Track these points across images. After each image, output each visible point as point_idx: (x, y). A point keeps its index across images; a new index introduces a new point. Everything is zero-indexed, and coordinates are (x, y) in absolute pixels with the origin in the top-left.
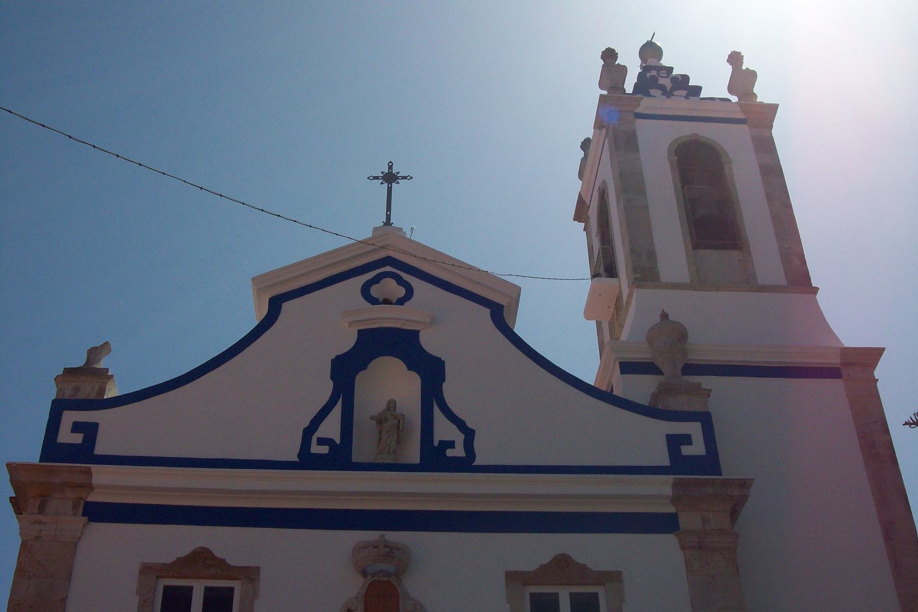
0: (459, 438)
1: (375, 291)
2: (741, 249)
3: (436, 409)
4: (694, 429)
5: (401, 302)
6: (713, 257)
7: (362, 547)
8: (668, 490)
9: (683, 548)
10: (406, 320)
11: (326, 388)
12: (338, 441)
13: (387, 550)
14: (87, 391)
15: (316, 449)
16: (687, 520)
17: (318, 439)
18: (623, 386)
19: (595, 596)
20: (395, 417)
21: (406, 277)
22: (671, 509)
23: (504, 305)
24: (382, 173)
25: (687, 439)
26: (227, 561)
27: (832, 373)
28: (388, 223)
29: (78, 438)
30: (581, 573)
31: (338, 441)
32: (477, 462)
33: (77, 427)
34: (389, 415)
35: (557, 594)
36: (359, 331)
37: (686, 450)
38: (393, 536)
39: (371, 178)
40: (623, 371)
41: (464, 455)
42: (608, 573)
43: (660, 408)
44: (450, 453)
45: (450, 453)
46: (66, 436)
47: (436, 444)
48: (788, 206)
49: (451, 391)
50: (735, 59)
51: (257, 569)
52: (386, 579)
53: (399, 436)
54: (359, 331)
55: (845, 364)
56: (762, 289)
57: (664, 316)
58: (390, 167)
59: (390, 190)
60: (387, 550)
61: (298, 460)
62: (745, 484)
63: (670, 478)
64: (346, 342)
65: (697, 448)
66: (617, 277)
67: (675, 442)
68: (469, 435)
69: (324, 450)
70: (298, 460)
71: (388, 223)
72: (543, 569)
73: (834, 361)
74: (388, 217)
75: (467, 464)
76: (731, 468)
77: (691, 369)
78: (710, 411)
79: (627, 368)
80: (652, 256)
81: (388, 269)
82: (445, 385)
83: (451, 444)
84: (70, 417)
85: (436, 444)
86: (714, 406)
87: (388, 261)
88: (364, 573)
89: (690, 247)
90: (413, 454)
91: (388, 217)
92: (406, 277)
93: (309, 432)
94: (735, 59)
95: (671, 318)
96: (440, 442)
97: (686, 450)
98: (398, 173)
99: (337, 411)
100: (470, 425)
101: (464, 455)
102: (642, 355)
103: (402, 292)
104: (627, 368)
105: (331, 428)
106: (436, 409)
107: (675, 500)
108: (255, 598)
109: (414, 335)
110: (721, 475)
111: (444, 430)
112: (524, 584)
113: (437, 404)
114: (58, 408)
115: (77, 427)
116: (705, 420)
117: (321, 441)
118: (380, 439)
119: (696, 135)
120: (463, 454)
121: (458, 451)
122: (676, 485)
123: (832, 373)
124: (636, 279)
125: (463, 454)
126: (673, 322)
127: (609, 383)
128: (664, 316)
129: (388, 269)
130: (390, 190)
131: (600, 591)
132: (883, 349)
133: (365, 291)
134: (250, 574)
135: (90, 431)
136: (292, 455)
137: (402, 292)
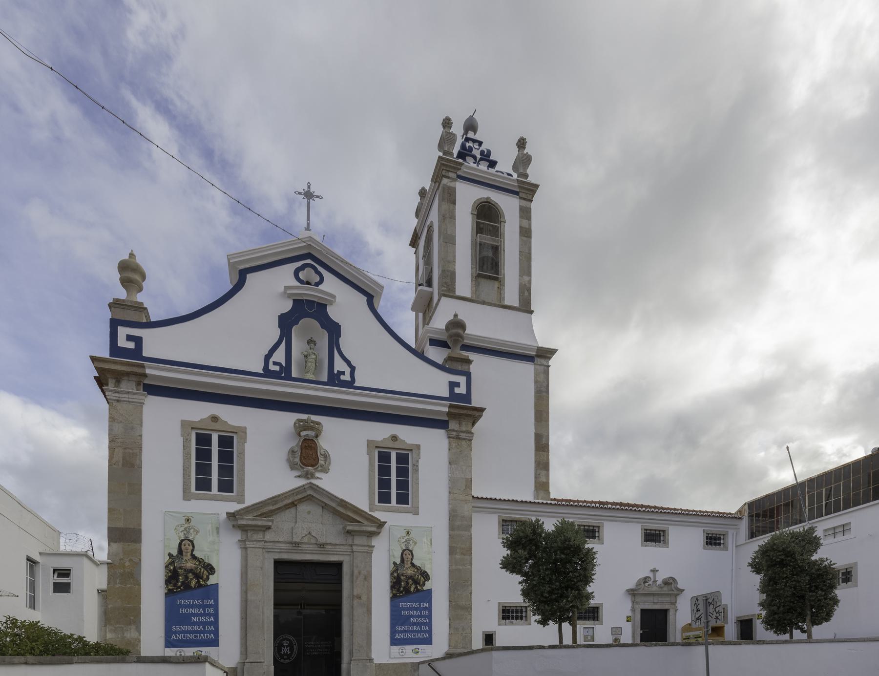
0: (348, 370)
4: (462, 380)
11: (276, 333)
12: (284, 365)
15: (272, 367)
22: (447, 419)
25: (458, 385)
29: (131, 345)
33: (129, 338)
37: (457, 390)
44: (342, 377)
45: (342, 377)
46: (122, 343)
47: (336, 372)
61: (263, 372)
65: (461, 390)
67: (453, 385)
68: (353, 369)
69: (277, 368)
70: (263, 372)
75: (350, 384)
83: (343, 373)
84: (123, 332)
85: (336, 372)
93: (268, 357)
96: (338, 371)
97: (457, 390)
99: (283, 346)
105: (280, 356)
111: (339, 365)
114: (114, 324)
115: (129, 338)
116: (468, 375)
117: (275, 363)
120: (350, 380)
121: (347, 377)
125: (350, 380)
135: (138, 341)
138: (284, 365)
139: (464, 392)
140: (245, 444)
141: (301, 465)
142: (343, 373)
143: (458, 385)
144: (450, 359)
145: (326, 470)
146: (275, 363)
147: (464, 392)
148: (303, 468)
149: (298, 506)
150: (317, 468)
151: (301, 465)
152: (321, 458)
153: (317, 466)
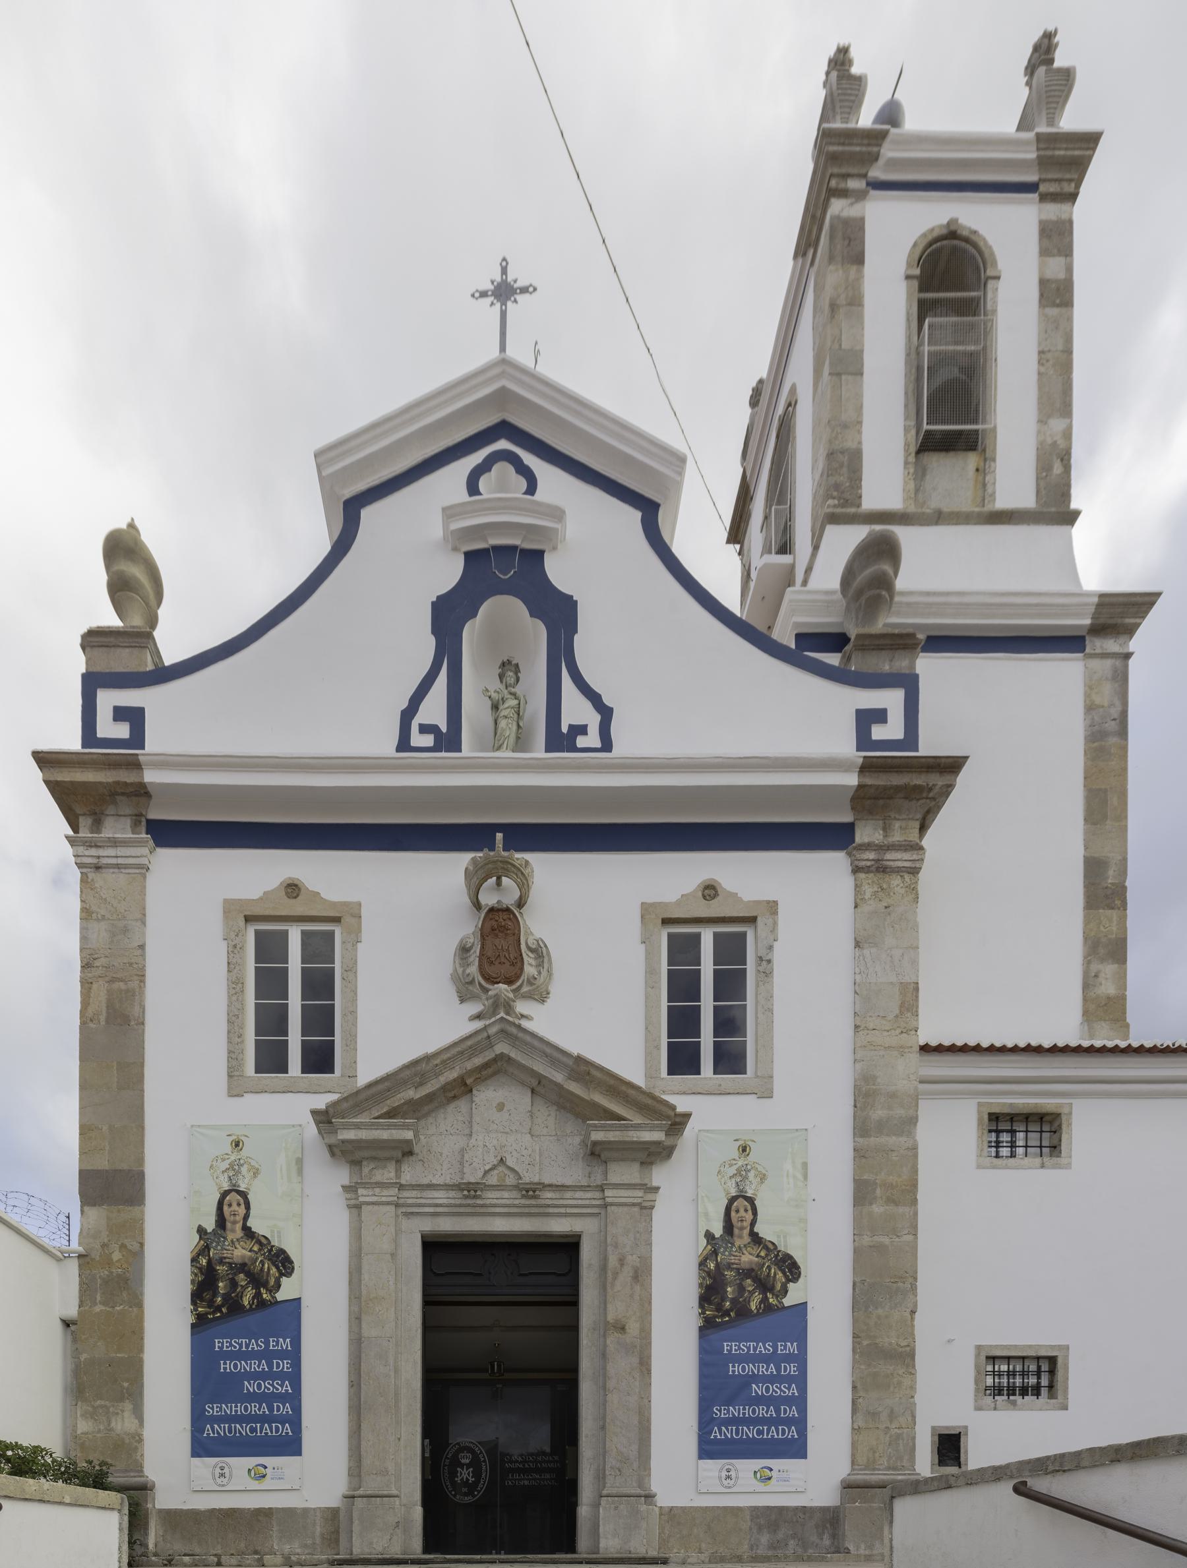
0: (593, 720)
11: (427, 646)
12: (444, 728)
14: (123, 660)
21: (529, 459)
25: (880, 716)
26: (322, 895)
31: (444, 729)
33: (120, 714)
37: (878, 733)
44: (581, 742)
47: (565, 729)
49: (584, 646)
59: (503, 315)
67: (867, 718)
68: (606, 713)
81: (503, 444)
82: (576, 637)
84: (107, 700)
85: (565, 729)
92: (529, 459)
93: (407, 715)
96: (571, 727)
97: (878, 733)
100: (607, 701)
114: (92, 683)
115: (120, 714)
117: (424, 729)
130: (503, 315)
132: (1158, 595)
138: (444, 729)
141: (483, 982)
142: (582, 730)
143: (880, 716)
145: (541, 996)
146: (424, 729)
148: (486, 991)
152: (528, 959)
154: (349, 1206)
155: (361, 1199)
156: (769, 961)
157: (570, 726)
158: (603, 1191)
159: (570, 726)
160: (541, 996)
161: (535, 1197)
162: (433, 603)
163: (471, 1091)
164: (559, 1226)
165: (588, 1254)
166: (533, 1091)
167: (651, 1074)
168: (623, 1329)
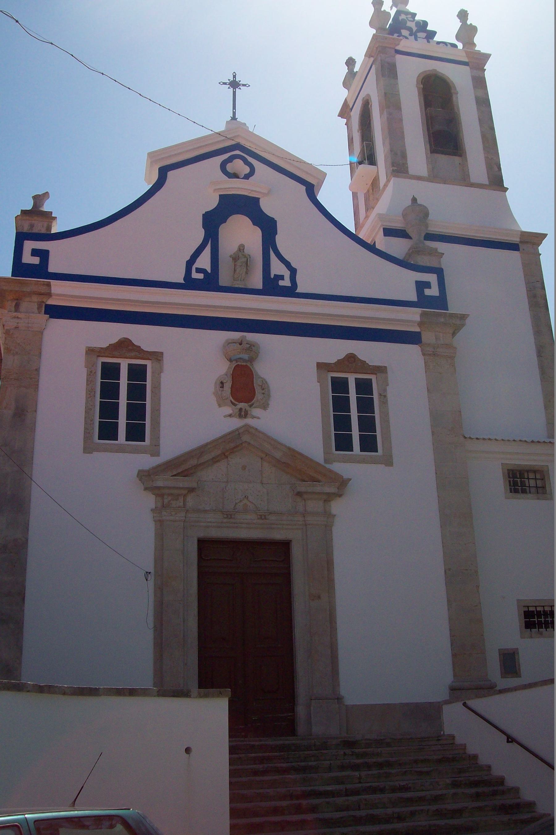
0: (287, 274)
1: (230, 167)
2: (460, 156)
3: (272, 253)
4: (432, 278)
5: (247, 177)
6: (443, 159)
7: (229, 343)
8: (417, 318)
9: (424, 354)
10: (252, 191)
11: (199, 235)
12: (209, 271)
13: (248, 346)
14: (39, 227)
15: (196, 275)
16: (427, 337)
17: (196, 268)
18: (382, 243)
19: (371, 380)
20: (245, 256)
21: (250, 159)
22: (417, 329)
23: (314, 184)
24: (229, 80)
25: (428, 285)
27: (512, 247)
28: (234, 118)
29: (36, 260)
30: (363, 366)
31: (209, 271)
32: (299, 290)
33: (35, 252)
34: (240, 255)
35: (347, 378)
36: (220, 196)
37: (427, 292)
38: (252, 337)
39: (222, 83)
40: (385, 235)
41: (290, 285)
42: (379, 367)
43: (412, 262)
45: (281, 283)
46: (28, 258)
47: (272, 276)
48: (492, 129)
49: (281, 240)
50: (463, 15)
51: (162, 353)
52: (245, 364)
53: (247, 269)
54: (220, 196)
55: (521, 242)
56: (472, 185)
57: (414, 200)
58: (234, 77)
60: (248, 346)
61: (184, 282)
62: (463, 317)
63: (418, 310)
64: (212, 203)
65: (433, 291)
66: (375, 165)
67: (421, 286)
68: (293, 272)
69: (201, 276)
70: (184, 282)
71: (234, 118)
72: (339, 362)
73: (516, 239)
74: (234, 113)
76: (454, 307)
77: (431, 237)
78: (443, 267)
79: (388, 232)
80: (404, 156)
81: (237, 152)
83: (282, 277)
84: (29, 246)
85: (272, 276)
86: (445, 263)
87: (238, 146)
88: (230, 360)
89: (429, 152)
90: (257, 282)
91: (234, 113)
92: (250, 159)
94: (463, 15)
95: (419, 202)
97: (427, 292)
98: (240, 81)
99: (208, 250)
100: (294, 265)
101: (290, 285)
102: (398, 224)
103: (247, 170)
104: (388, 232)
106: (272, 253)
107: (420, 324)
108: (161, 372)
109: (256, 201)
110: (448, 310)
111: (277, 268)
112: (328, 372)
113: (273, 251)
115: (35, 252)
116: (439, 272)
117: (199, 270)
118: (235, 270)
119: (435, 70)
121: (286, 283)
122: (423, 315)
123: (512, 247)
124: (393, 171)
126: (420, 205)
127: (373, 239)
128: (414, 200)
129: (237, 152)
131: (373, 377)
133: (223, 166)
134: (157, 357)
135: (44, 255)
136: (180, 279)
137: (247, 170)
138: (209, 271)
139: (437, 294)
140: (162, 375)
141: (233, 400)
142: (282, 277)
144: (415, 251)
145: (265, 406)
146: (199, 270)
147: (437, 294)
148: (235, 405)
149: (229, 459)
150: (253, 404)
151: (233, 400)
152: (258, 390)
153: (253, 402)
154: (155, 521)
155: (164, 518)
156: (385, 396)
157: (275, 275)
158: (304, 516)
159: (275, 275)
160: (265, 406)
161: (265, 519)
162: (203, 215)
163: (227, 457)
164: (278, 535)
165: (296, 552)
166: (262, 459)
167: (327, 452)
168: (319, 597)
